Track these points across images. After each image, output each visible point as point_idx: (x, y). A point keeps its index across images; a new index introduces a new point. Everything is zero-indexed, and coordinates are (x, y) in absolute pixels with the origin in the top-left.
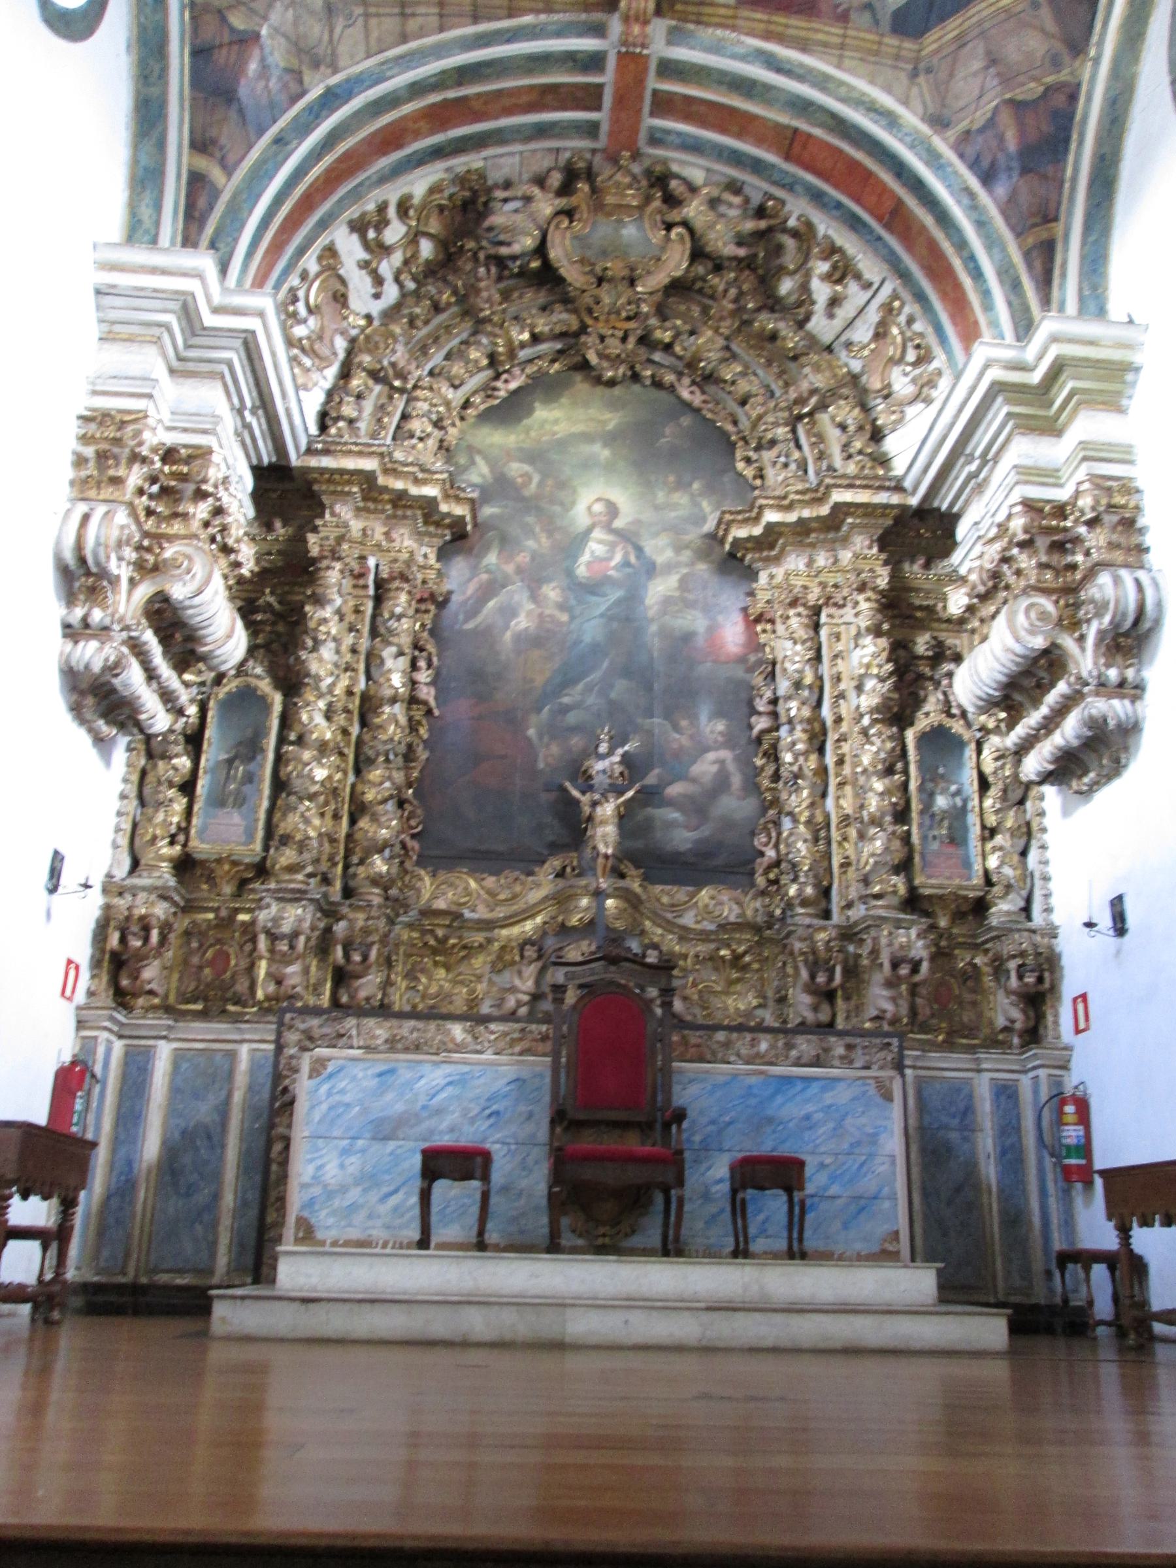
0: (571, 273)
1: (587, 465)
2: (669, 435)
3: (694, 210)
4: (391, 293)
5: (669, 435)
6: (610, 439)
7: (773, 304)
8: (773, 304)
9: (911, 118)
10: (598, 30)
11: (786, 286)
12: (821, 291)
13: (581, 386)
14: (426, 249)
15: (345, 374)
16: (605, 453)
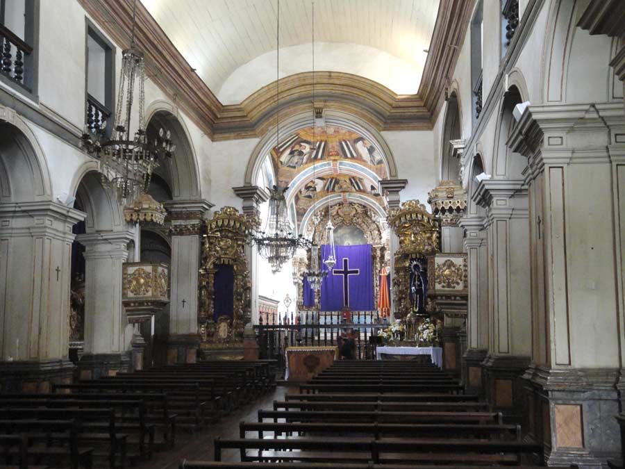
0: (342, 215)
1: (346, 238)
2: (356, 233)
3: (356, 206)
4: (319, 220)
5: (356, 233)
6: (349, 233)
7: (367, 216)
8: (367, 216)
9: (377, 204)
10: (340, 196)
11: (369, 213)
12: (373, 215)
13: (344, 226)
14: (323, 213)
15: (315, 232)
16: (347, 236)
